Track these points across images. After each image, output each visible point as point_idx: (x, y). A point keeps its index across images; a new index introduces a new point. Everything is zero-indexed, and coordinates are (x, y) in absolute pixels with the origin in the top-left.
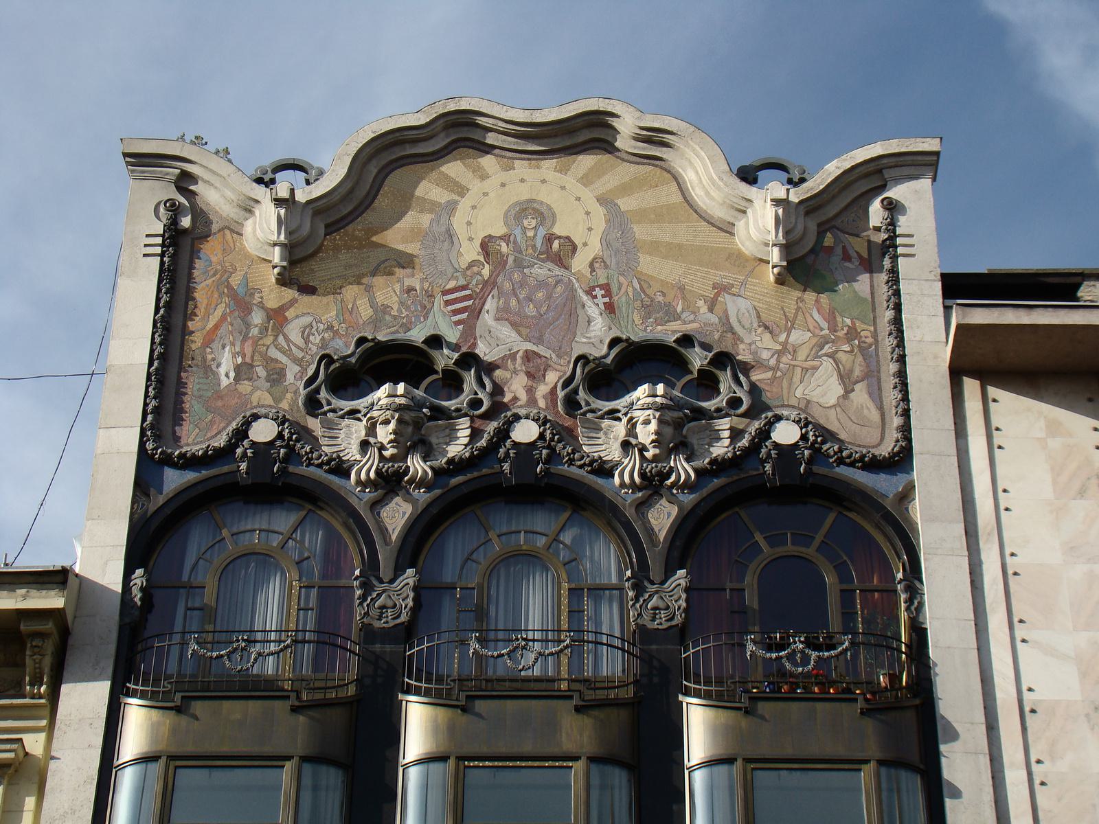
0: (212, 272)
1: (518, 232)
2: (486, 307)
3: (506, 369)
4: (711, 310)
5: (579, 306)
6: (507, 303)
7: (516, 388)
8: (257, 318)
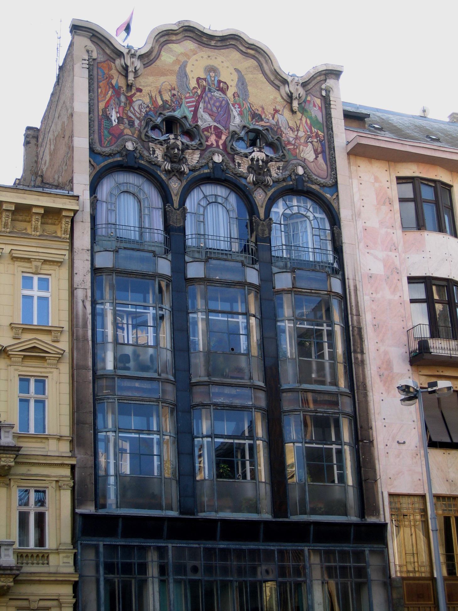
0: (105, 78)
1: (209, 77)
2: (200, 106)
3: (208, 132)
4: (273, 119)
5: (231, 111)
6: (207, 106)
7: (213, 139)
8: (123, 99)
